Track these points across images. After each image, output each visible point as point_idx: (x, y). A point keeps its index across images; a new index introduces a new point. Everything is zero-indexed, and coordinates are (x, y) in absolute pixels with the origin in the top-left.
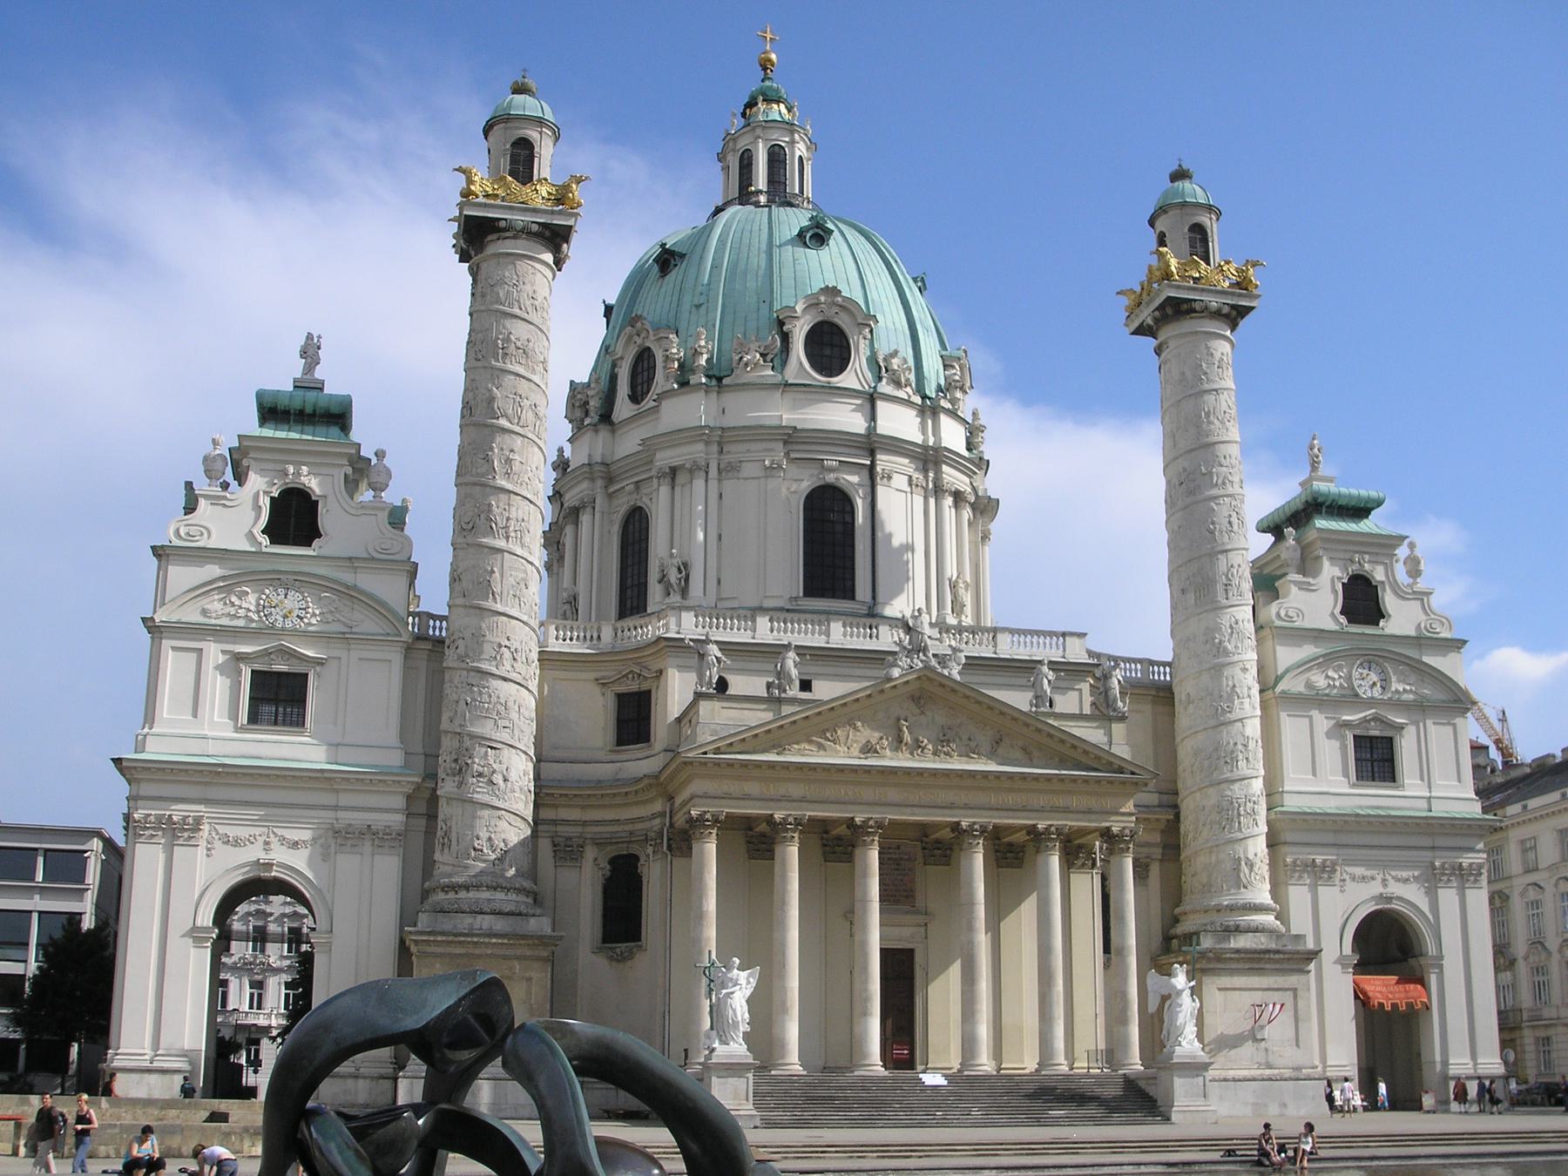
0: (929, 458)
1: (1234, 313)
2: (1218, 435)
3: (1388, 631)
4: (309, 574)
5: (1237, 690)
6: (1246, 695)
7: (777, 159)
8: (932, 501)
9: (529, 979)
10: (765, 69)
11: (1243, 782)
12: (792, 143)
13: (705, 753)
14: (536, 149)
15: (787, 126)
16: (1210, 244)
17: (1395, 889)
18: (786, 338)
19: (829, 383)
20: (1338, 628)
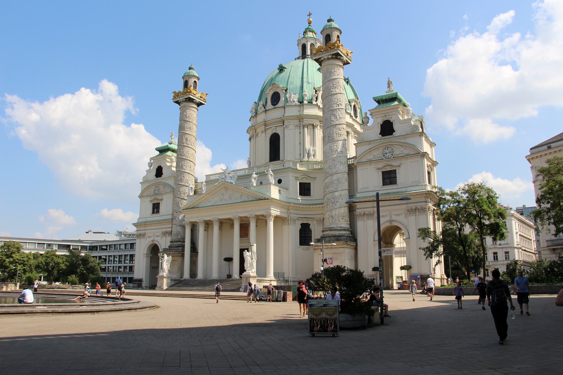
0: (300, 118)
1: (334, 56)
2: (328, 94)
3: (396, 135)
4: (159, 183)
5: (330, 167)
6: (333, 168)
7: (304, 47)
8: (302, 129)
9: (178, 260)
10: (309, 24)
11: (331, 193)
12: (307, 41)
13: (184, 209)
14: (188, 82)
15: (305, 38)
16: (331, 38)
17: (394, 218)
18: (267, 99)
19: (274, 107)
20: (379, 138)
